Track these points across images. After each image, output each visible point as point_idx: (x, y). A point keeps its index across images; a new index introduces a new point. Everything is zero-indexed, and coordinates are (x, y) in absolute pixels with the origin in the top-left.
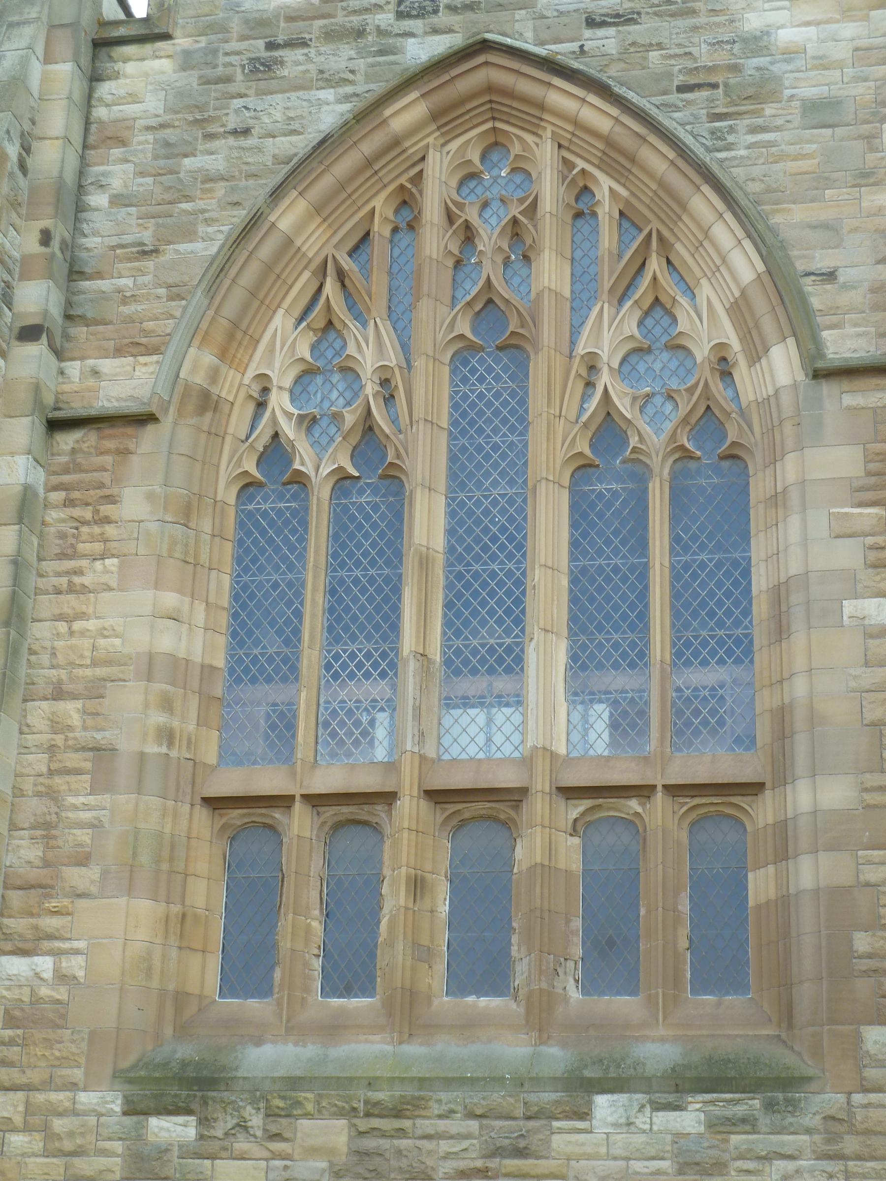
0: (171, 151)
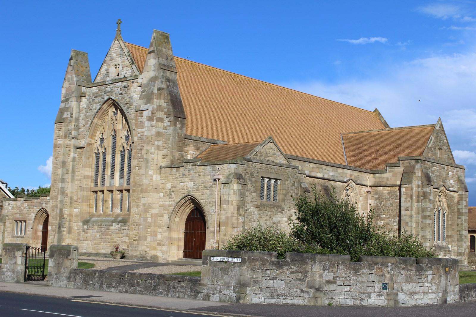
0: (87, 112)
